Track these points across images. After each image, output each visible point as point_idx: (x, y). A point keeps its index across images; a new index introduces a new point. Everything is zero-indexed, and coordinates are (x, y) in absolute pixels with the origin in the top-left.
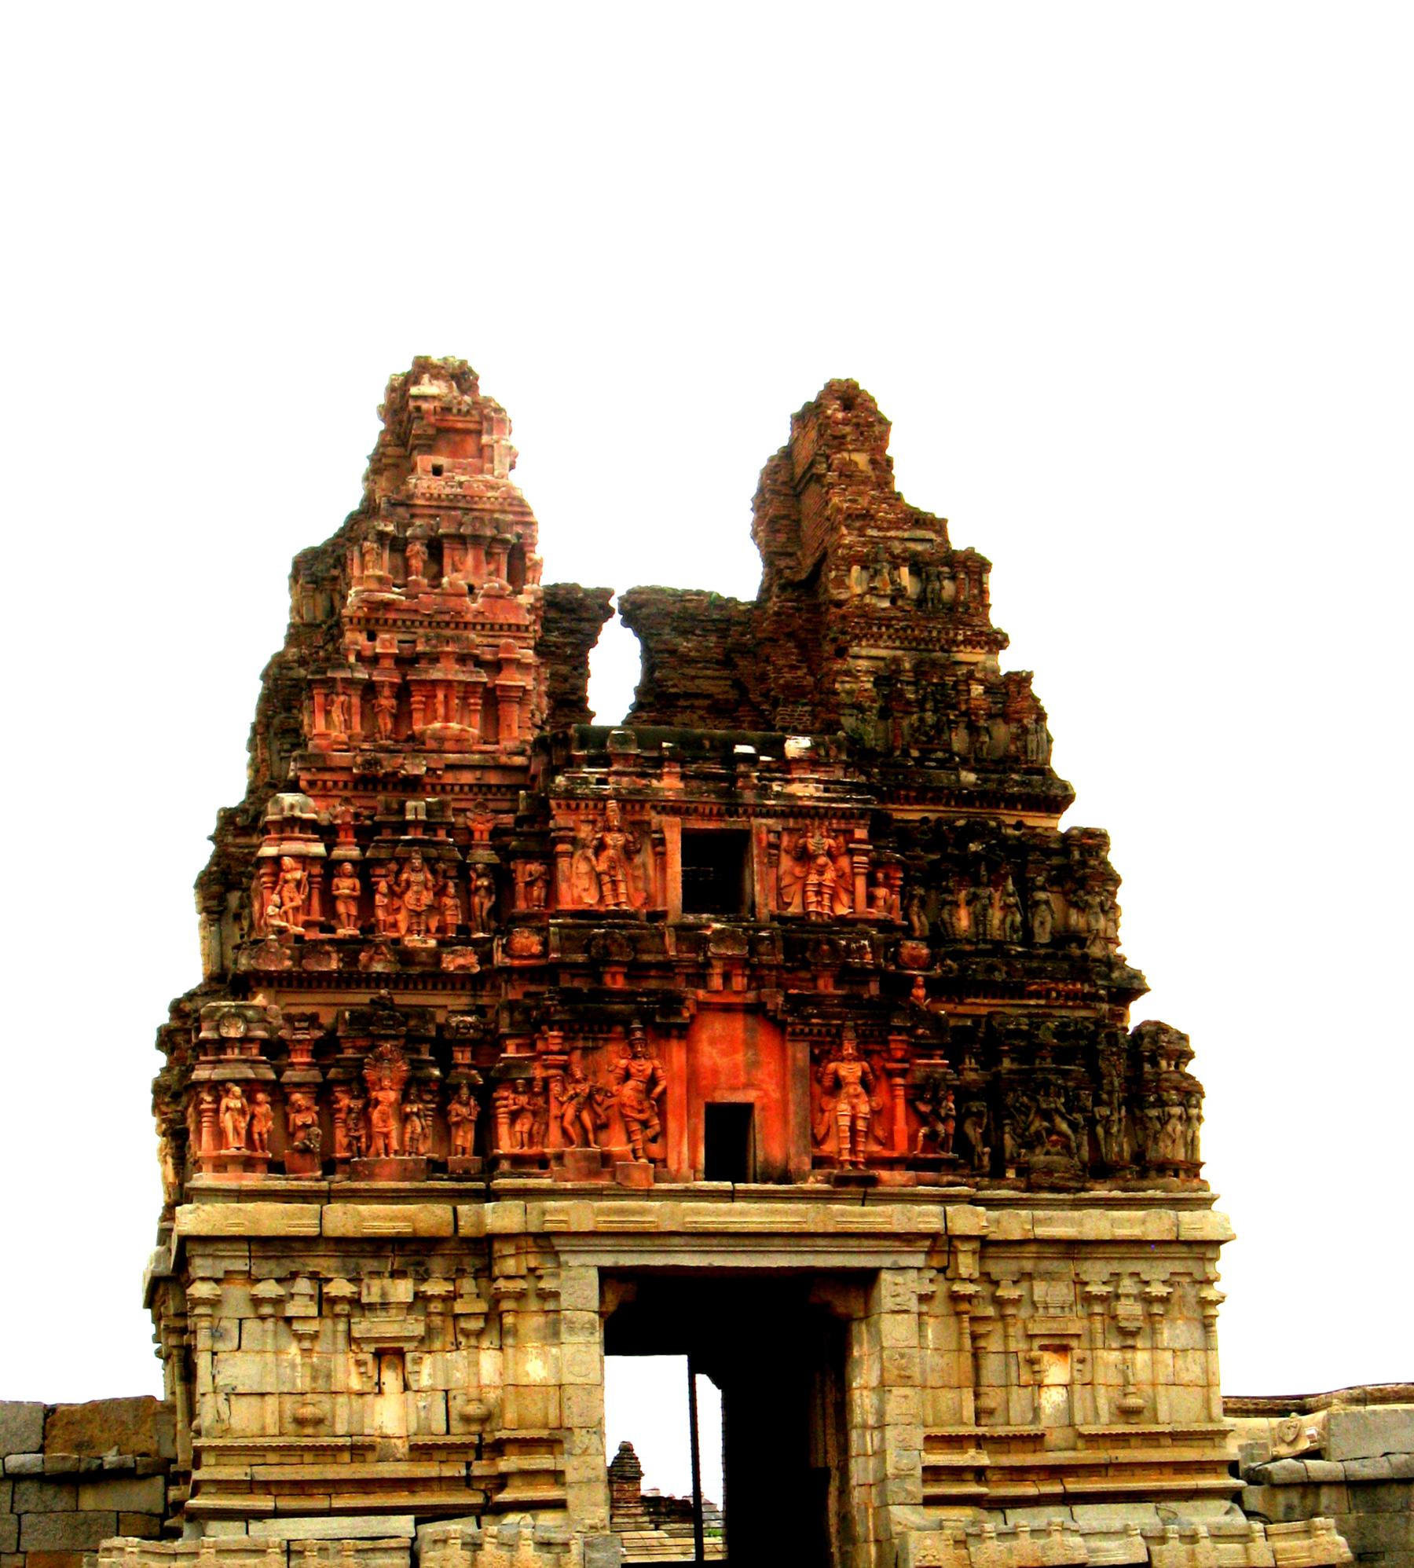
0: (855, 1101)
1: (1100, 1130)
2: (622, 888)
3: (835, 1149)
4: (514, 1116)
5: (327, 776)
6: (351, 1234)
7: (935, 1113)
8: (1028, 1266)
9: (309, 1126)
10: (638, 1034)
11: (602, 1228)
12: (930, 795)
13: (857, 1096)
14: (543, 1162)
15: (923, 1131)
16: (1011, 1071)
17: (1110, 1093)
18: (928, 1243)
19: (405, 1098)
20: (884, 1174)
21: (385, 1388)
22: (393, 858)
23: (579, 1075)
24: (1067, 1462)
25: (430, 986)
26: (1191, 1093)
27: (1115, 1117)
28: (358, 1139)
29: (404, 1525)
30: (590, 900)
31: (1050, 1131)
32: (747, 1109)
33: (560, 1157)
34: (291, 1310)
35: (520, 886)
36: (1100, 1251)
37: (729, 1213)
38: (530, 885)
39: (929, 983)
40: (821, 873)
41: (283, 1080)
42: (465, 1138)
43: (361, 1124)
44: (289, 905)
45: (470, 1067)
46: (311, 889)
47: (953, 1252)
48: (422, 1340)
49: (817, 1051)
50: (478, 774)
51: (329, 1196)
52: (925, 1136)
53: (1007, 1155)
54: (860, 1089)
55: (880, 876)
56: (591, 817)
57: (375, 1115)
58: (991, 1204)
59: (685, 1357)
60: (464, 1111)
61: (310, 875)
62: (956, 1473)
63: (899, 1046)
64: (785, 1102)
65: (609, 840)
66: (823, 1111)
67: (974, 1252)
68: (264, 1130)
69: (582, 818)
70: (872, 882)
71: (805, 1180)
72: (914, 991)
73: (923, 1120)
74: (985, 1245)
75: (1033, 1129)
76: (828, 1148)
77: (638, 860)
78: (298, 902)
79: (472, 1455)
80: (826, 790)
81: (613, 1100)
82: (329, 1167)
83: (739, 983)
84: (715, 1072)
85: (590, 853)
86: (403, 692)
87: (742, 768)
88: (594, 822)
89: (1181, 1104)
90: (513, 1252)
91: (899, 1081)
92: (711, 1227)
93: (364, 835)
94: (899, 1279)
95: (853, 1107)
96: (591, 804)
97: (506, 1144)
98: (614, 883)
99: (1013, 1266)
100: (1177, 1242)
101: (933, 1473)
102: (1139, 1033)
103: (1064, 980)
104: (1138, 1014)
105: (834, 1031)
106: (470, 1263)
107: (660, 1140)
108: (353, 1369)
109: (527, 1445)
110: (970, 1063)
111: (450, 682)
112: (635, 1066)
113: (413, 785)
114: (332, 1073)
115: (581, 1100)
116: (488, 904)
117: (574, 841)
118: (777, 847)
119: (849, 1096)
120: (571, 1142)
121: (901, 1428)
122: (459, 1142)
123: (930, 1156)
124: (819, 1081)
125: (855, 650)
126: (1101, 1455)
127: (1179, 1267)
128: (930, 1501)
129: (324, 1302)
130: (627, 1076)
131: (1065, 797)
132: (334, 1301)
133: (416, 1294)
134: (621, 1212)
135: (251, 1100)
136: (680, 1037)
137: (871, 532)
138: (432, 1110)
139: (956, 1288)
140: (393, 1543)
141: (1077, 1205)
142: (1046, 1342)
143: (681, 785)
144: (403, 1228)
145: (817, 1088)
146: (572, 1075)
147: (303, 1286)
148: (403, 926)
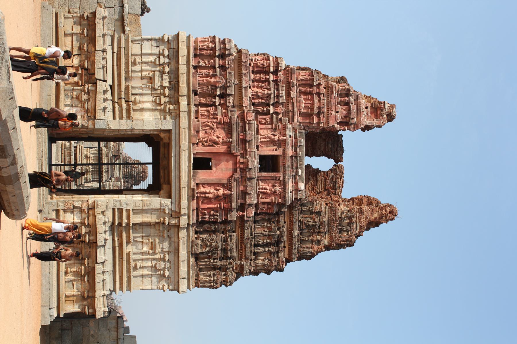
2: (265, 140)
4: (208, 111)
7: (211, 215)
8: (173, 239)
11: (181, 129)
16: (222, 237)
18: (178, 211)
19: (212, 86)
20: (195, 201)
29: (110, 82)
33: (198, 121)
35: (264, 117)
36: (176, 258)
37: (185, 161)
38: (265, 119)
42: (203, 101)
44: (258, 62)
45: (220, 102)
48: (154, 89)
51: (188, 67)
55: (270, 206)
57: (208, 79)
59: (151, 183)
62: (120, 218)
65: (276, 137)
70: (268, 203)
71: (194, 180)
78: (259, 64)
79: (127, 100)
80: (291, 192)
82: (195, 67)
93: (276, 82)
94: (170, 203)
97: (201, 109)
100: (179, 278)
101: (120, 211)
106: (172, 100)
108: (147, 73)
109: (128, 111)
111: (314, 104)
113: (288, 94)
114: (218, 69)
116: (260, 110)
118: (276, 180)
125: (327, 207)
127: (173, 279)
128: (114, 210)
129: (163, 65)
130: (218, 138)
132: (163, 68)
133: (165, 87)
134: (185, 134)
137: (358, 214)
140: (105, 76)
141: (188, 252)
142: (154, 243)
147: (167, 60)
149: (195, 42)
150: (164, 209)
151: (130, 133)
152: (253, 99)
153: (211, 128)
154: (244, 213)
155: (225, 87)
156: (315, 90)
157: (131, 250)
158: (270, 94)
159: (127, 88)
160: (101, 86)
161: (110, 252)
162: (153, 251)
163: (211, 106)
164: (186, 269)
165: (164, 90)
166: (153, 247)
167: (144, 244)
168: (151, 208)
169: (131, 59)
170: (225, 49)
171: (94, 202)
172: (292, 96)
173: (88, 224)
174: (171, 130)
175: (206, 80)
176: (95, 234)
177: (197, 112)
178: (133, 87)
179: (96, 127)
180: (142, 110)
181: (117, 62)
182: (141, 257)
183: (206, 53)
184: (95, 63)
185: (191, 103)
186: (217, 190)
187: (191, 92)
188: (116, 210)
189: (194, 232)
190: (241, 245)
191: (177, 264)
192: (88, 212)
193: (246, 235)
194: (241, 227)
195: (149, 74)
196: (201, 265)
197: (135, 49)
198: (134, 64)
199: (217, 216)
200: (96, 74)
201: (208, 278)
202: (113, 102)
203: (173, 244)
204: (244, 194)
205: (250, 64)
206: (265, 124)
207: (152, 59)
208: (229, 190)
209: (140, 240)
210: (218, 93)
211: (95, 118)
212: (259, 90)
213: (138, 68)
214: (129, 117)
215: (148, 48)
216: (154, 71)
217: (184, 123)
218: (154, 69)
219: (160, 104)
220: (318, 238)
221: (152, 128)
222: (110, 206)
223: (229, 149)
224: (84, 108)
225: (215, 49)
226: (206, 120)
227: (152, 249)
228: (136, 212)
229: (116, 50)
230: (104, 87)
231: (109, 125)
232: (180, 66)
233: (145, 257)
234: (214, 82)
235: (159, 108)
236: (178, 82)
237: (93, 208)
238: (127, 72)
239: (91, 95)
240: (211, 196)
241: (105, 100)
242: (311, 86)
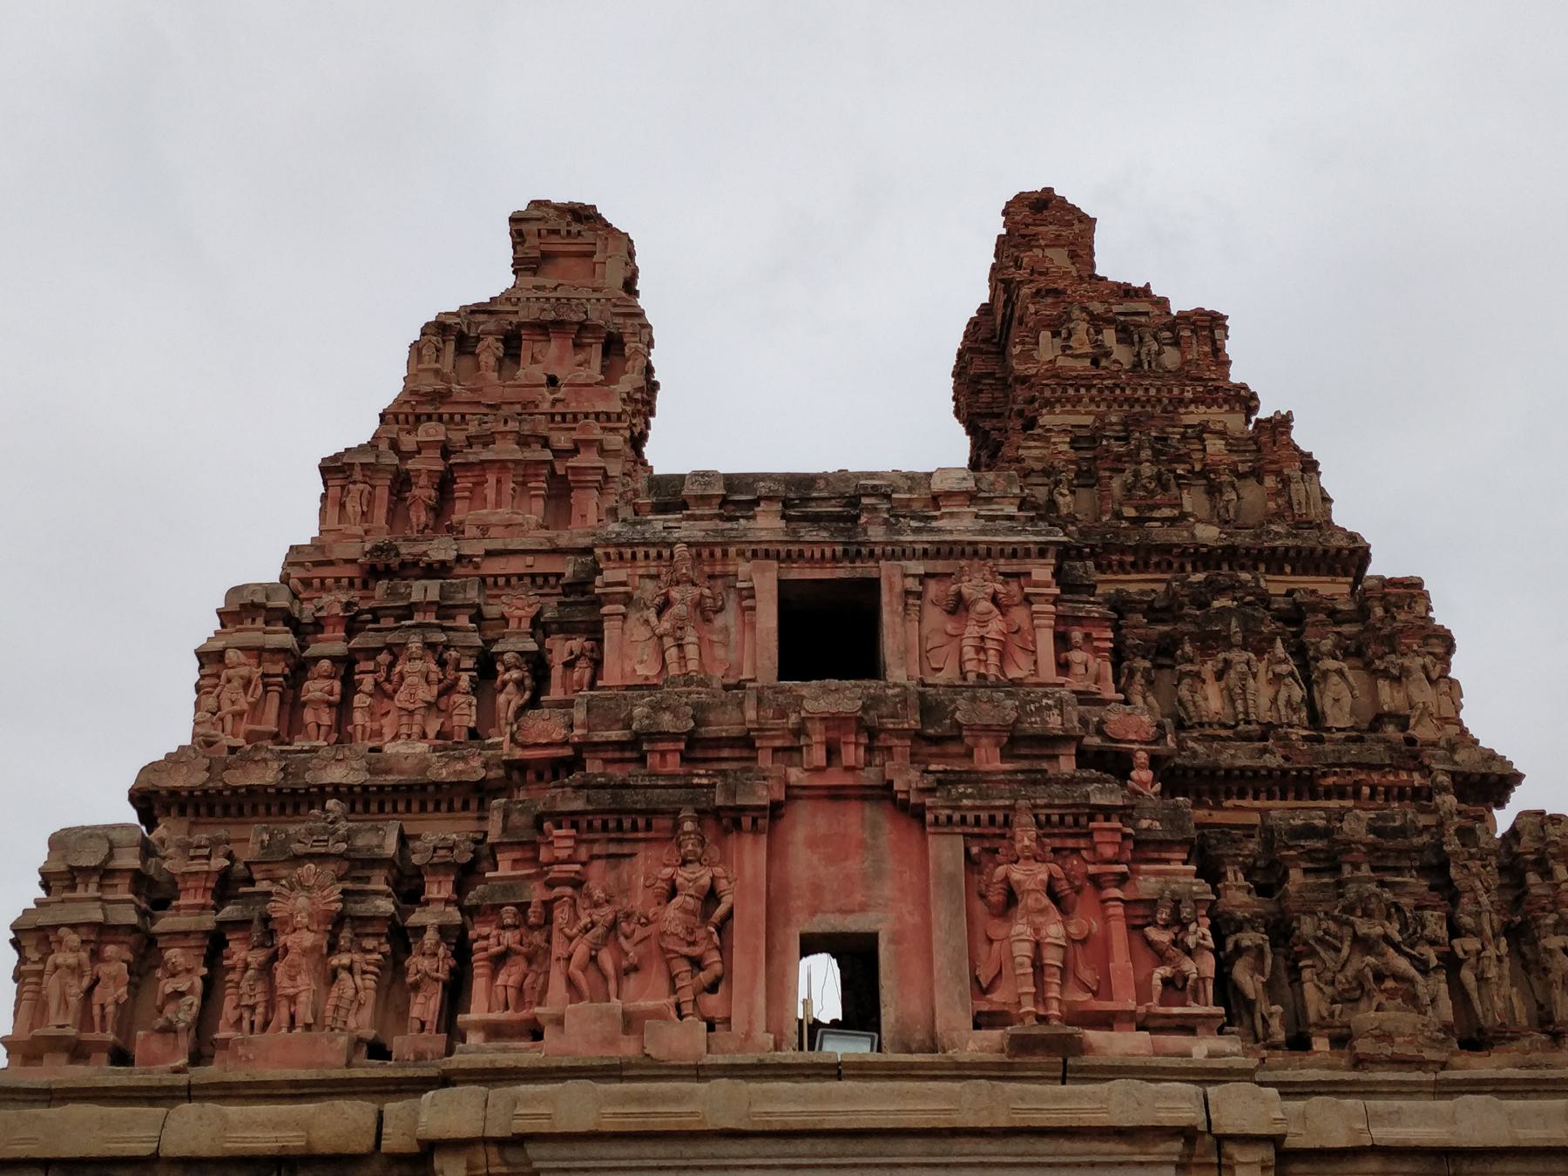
0: (1039, 919)
1: (1467, 975)
2: (691, 651)
3: (1012, 999)
4: (499, 961)
7: (1174, 943)
9: (182, 994)
10: (688, 826)
13: (1042, 911)
14: (537, 1035)
15: (1165, 971)
17: (1478, 914)
22: (389, 647)
23: (598, 894)
27: (1491, 951)
28: (252, 1008)
30: (646, 670)
31: (1379, 977)
32: (873, 938)
38: (569, 665)
40: (983, 624)
41: (157, 928)
42: (426, 1006)
43: (260, 987)
45: (447, 902)
49: (975, 850)
52: (1166, 982)
53: (1312, 1016)
54: (1046, 901)
56: (653, 571)
57: (280, 968)
60: (425, 964)
63: (1108, 837)
64: (927, 926)
65: (675, 593)
66: (991, 941)
68: (110, 999)
69: (640, 571)
72: (1133, 774)
73: (1161, 957)
75: (1350, 972)
76: (999, 997)
77: (719, 621)
81: (651, 929)
82: (197, 1058)
83: (851, 754)
84: (816, 889)
85: (651, 614)
88: (656, 577)
95: (1037, 930)
96: (653, 552)
97: (478, 1011)
98: (680, 646)
103: (1371, 767)
107: (721, 988)
110: (1234, 876)
112: (683, 875)
114: (230, 911)
115: (599, 930)
116: (517, 701)
117: (628, 599)
119: (1029, 912)
120: (581, 998)
122: (415, 1011)
123: (1176, 1010)
130: (673, 892)
135: (96, 956)
136: (755, 829)
138: (376, 964)
143: (782, 524)
145: (979, 906)
146: (589, 896)
177: (494, 1031)
185: (433, 1072)
189: (1297, 1057)
204: (1015, 742)
206: (597, 664)
208: (1007, 823)
210: (386, 906)
223: (746, 822)
225: (91, 925)
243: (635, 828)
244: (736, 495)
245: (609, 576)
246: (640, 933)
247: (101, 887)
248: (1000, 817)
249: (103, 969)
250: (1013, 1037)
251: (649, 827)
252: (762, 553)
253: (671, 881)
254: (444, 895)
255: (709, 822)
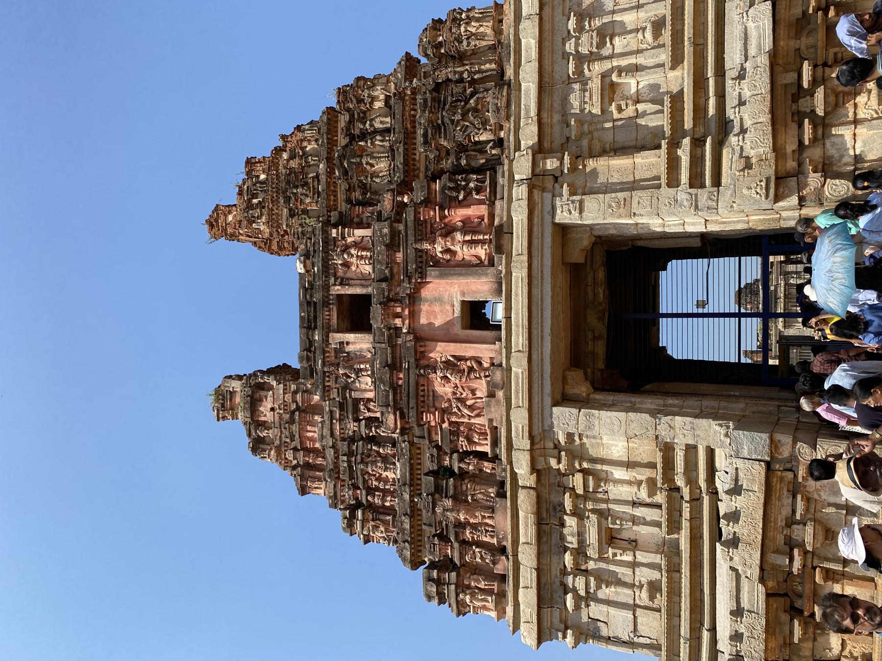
2: (362, 366)
4: (470, 441)
5: (338, 494)
6: (536, 552)
7: (465, 188)
8: (557, 117)
11: (526, 405)
12: (332, 188)
17: (455, 72)
18: (535, 191)
20: (496, 222)
21: (633, 538)
23: (446, 405)
24: (692, 77)
25: (419, 467)
26: (455, 18)
32: (463, 302)
34: (582, 593)
35: (372, 415)
38: (369, 410)
39: (402, 194)
40: (352, 256)
42: (487, 467)
44: (384, 535)
46: (379, 519)
47: (545, 173)
48: (600, 513)
50: (334, 421)
51: (515, 555)
52: (477, 194)
53: (492, 137)
57: (472, 521)
58: (518, 148)
61: (373, 520)
62: (696, 161)
67: (545, 158)
70: (360, 225)
73: (470, 193)
74: (540, 150)
78: (382, 529)
79: (675, 494)
82: (503, 550)
86: (308, 451)
87: (308, 297)
89: (460, 25)
90: (543, 459)
91: (446, 211)
92: (526, 335)
93: (355, 487)
97: (487, 449)
99: (557, 129)
100: (540, 15)
101: (696, 181)
102: (426, 55)
104: (424, 60)
105: (420, 254)
115: (459, 405)
121: (661, 206)
124: (448, 261)
126: (688, 49)
128: (717, 182)
129: (579, 571)
131: (329, 114)
132: (576, 563)
133: (573, 514)
134: (517, 392)
139: (566, 171)
142: (606, 100)
144: (532, 519)
145: (452, 263)
148: (393, 476)
149: (501, 613)
150: (572, 193)
151: (670, 401)
152: (394, 456)
153: (462, 401)
154: (399, 199)
155: (439, 491)
156: (301, 457)
157: (672, 74)
158: (362, 462)
159: (674, 526)
160: (748, 558)
161: (733, 58)
162: (607, 80)
163: (467, 454)
164: (523, 41)
165: (575, 506)
166: (610, 90)
167: (635, 97)
168: (608, 196)
169: (661, 601)
170: (439, 582)
171: (777, 198)
172: (332, 451)
173: (801, 125)
174: (556, 404)
175: (476, 517)
176: (779, 91)
177: (495, 443)
178: (658, 524)
179: (765, 436)
180: (629, 465)
181: (702, 601)
182: (640, 60)
183: (478, 581)
184: (767, 631)
185: (508, 467)
186: (447, 251)
187: (508, 494)
188: (708, 182)
189: (506, 144)
190: (414, 127)
191: (546, 52)
192: (800, 165)
193: (401, 150)
194: (414, 170)
195: (615, 555)
196: (490, 62)
197: (652, 626)
198: (654, 588)
199: (450, 189)
200: (762, 597)
201: (473, 30)
202: (714, 493)
203: (557, 105)
205: (398, 533)
206: (369, 400)
207: (606, 592)
208: (421, 251)
209: (641, 107)
211: (768, 464)
212: (385, 474)
213: (644, 575)
214: (668, 450)
215: (618, 622)
216: (601, 559)
217: (520, 419)
218: (602, 565)
219: (585, 472)
220: (294, 164)
221: (604, 414)
222: (726, 193)
224: (808, 500)
226: (473, 421)
227: (613, 85)
228: (652, 184)
229: (706, 635)
230: (736, 558)
231: (727, 435)
232: (535, 564)
233: (632, 60)
234: (458, 511)
235: (585, 465)
236: (540, 523)
237: (781, 178)
238: (674, 569)
239: (780, 539)
240: (459, 236)
241: (734, 516)
242: (308, 466)
243: (423, 391)
244: (308, 347)
245: (335, 395)
246: (460, 389)
247: (444, 584)
248: (420, 254)
249: (473, 584)
250: (496, 253)
251: (423, 385)
252: (326, 340)
253: (442, 378)
254: (448, 459)
255: (423, 362)
